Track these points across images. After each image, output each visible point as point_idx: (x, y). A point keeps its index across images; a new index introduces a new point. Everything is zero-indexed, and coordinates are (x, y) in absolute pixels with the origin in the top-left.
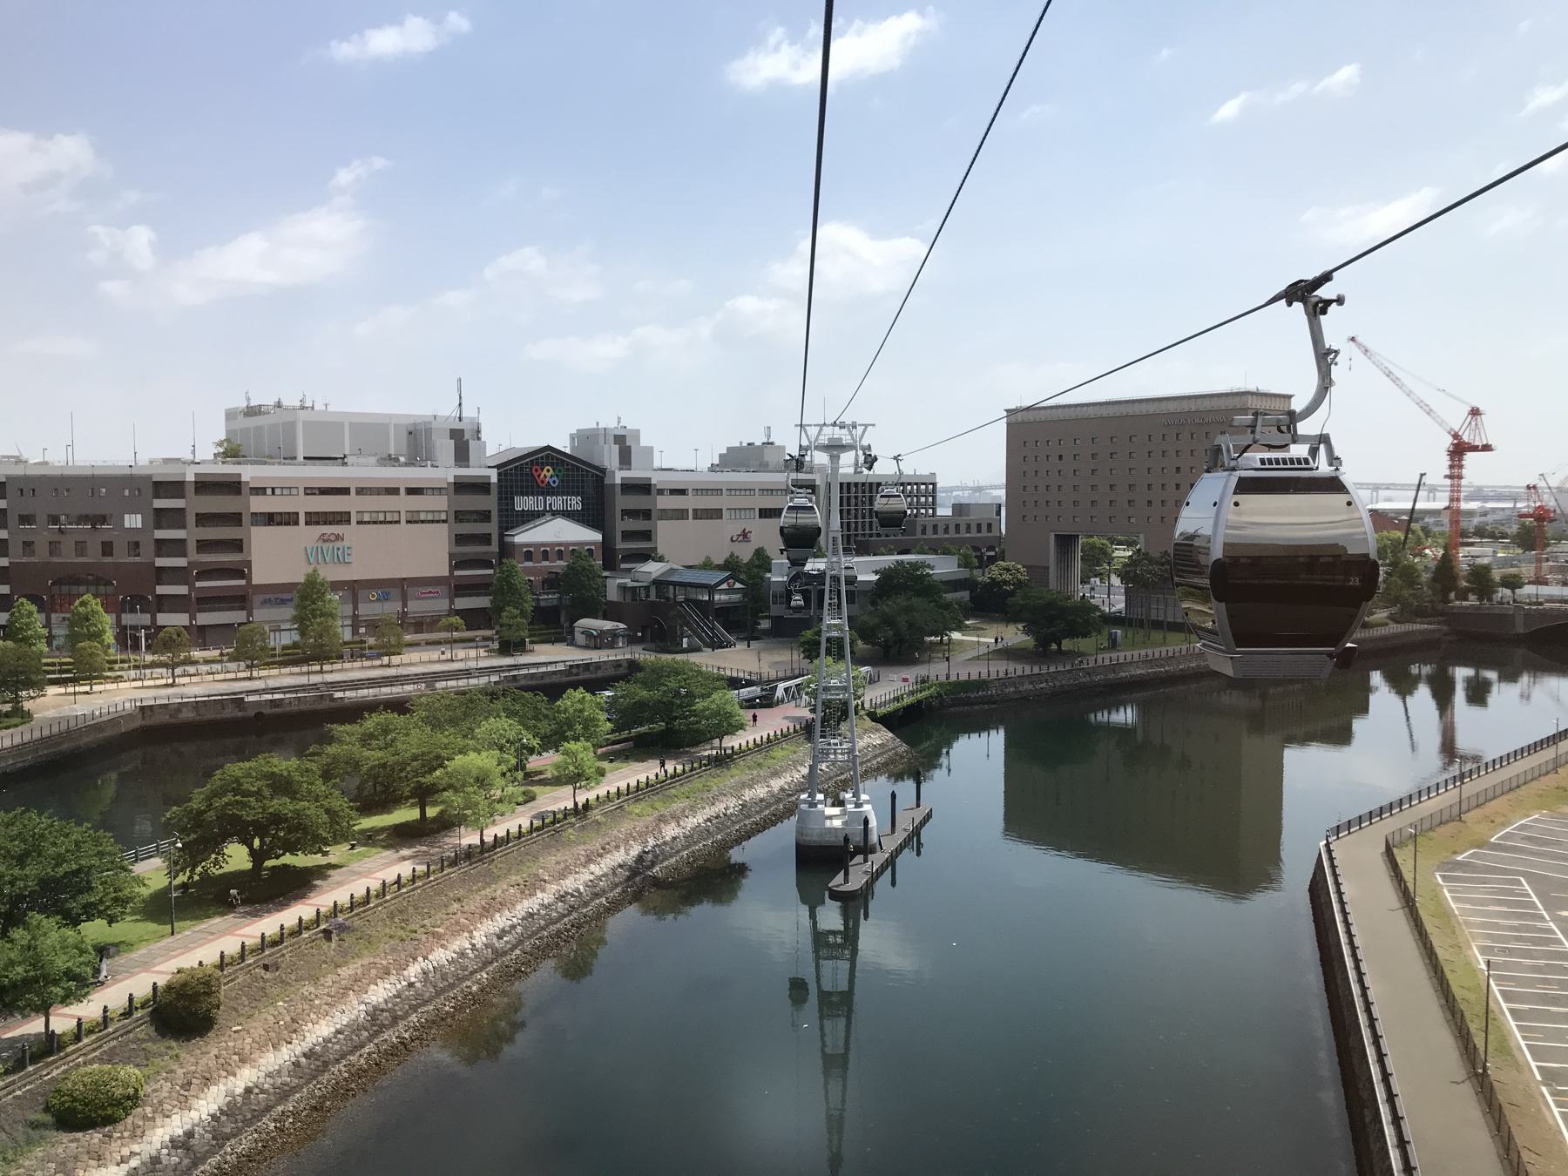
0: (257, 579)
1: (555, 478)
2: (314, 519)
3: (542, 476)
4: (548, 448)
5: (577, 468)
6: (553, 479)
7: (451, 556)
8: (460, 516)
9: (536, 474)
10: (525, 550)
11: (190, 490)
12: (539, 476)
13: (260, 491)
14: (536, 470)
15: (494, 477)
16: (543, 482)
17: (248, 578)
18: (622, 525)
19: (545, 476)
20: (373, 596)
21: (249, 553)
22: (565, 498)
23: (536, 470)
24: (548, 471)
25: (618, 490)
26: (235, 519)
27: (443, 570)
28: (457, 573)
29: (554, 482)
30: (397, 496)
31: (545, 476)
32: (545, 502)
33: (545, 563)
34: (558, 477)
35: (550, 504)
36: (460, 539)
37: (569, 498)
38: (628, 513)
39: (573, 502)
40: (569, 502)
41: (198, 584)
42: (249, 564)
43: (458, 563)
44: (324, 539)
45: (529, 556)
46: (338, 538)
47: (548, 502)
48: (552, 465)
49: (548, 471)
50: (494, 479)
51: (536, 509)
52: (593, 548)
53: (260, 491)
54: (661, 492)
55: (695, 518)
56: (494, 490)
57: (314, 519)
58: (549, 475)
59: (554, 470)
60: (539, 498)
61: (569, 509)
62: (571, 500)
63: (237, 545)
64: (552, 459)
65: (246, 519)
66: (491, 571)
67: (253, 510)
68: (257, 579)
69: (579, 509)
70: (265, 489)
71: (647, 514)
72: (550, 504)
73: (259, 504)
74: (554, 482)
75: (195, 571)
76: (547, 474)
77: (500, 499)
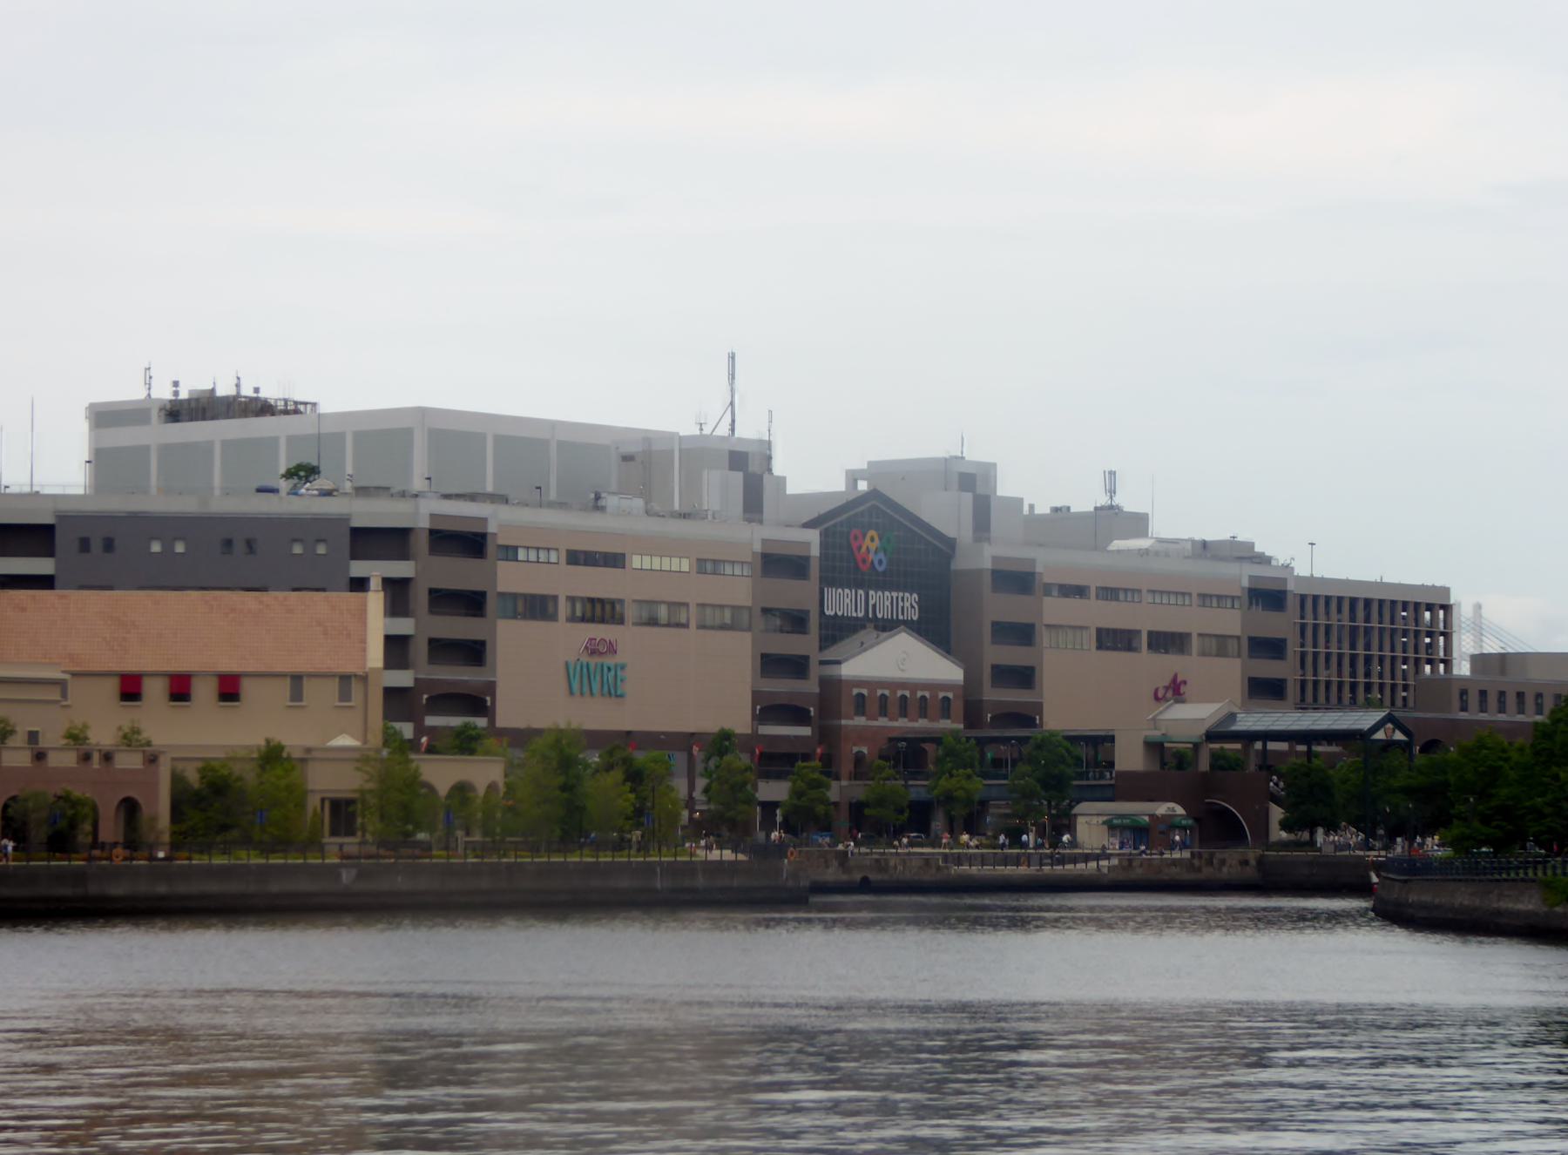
0: (501, 723)
1: (881, 555)
3: (863, 550)
7: (756, 696)
10: (855, 691)
11: (421, 544)
12: (860, 548)
13: (510, 552)
16: (864, 561)
21: (495, 676)
24: (872, 539)
27: (739, 720)
29: (880, 562)
31: (868, 548)
33: (883, 722)
37: (901, 594)
40: (901, 604)
41: (431, 721)
42: (491, 687)
43: (769, 710)
44: (593, 650)
45: (861, 705)
47: (871, 602)
50: (815, 551)
52: (950, 695)
54: (1047, 589)
58: (873, 546)
62: (903, 600)
63: (474, 652)
65: (491, 604)
66: (805, 731)
68: (501, 723)
69: (915, 618)
70: (515, 549)
72: (874, 606)
74: (880, 562)
75: (425, 696)
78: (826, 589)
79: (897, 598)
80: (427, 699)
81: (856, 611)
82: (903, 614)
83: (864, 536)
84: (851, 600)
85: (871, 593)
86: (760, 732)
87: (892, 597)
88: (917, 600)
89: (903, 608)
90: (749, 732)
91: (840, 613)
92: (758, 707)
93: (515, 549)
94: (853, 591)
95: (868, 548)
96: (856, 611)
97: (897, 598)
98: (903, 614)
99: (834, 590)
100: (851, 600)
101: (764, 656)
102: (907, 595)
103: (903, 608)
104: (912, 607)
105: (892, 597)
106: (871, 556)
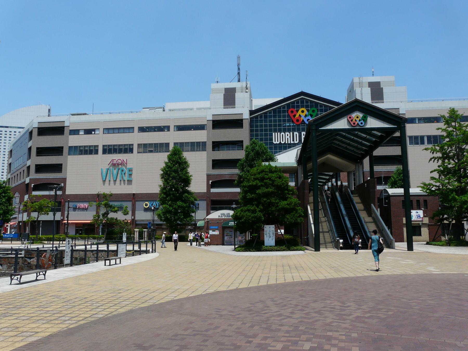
0: (69, 191)
2: (108, 150)
4: (302, 93)
7: (209, 177)
8: (217, 145)
9: (291, 115)
12: (295, 116)
14: (292, 112)
15: (246, 116)
17: (63, 189)
20: (146, 205)
23: (292, 112)
24: (303, 112)
26: (58, 151)
28: (213, 190)
31: (300, 115)
32: (300, 136)
36: (217, 164)
41: (34, 193)
42: (64, 180)
44: (114, 165)
46: (123, 163)
48: (307, 107)
51: (292, 142)
53: (75, 132)
56: (246, 124)
57: (108, 150)
58: (303, 115)
59: (308, 111)
60: (295, 133)
63: (58, 168)
64: (307, 102)
65: (66, 151)
67: (70, 145)
68: (69, 191)
73: (74, 141)
75: (33, 185)
76: (301, 114)
77: (251, 131)
78: (274, 134)
80: (33, 186)
81: (293, 140)
83: (297, 111)
84: (290, 137)
86: (211, 191)
90: (205, 191)
91: (282, 142)
92: (211, 181)
94: (291, 133)
95: (300, 115)
96: (293, 140)
99: (279, 133)
100: (290, 137)
101: (213, 161)
106: (302, 119)
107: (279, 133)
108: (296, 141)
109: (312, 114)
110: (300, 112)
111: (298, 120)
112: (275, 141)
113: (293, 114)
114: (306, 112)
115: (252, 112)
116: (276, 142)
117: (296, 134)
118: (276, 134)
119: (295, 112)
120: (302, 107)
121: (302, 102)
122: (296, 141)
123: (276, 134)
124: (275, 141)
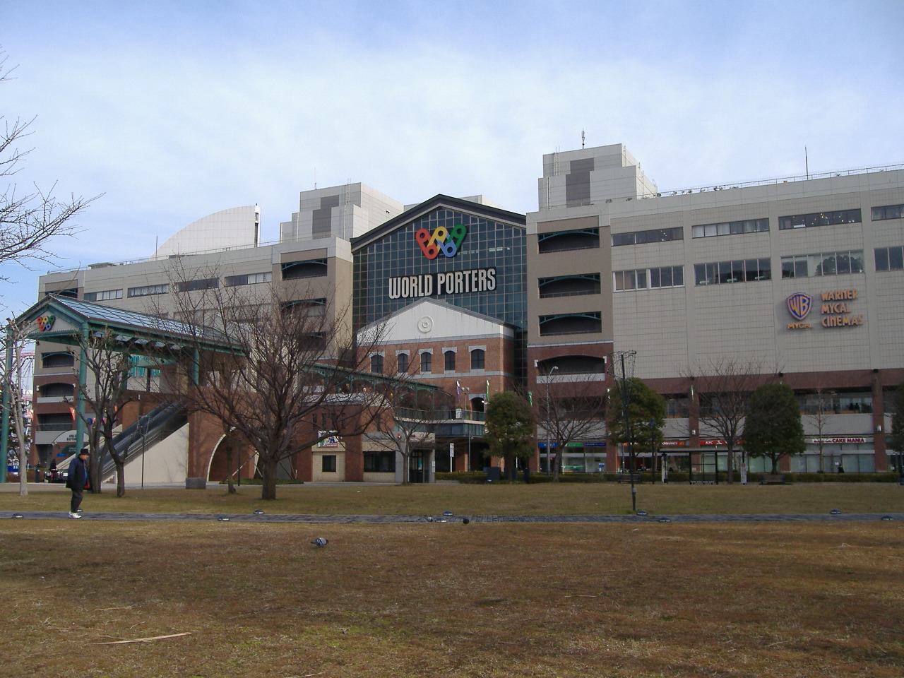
1: (451, 244)
3: (431, 243)
4: (440, 198)
5: (491, 223)
6: (448, 245)
12: (426, 243)
13: (91, 297)
18: (538, 307)
19: (435, 241)
22: (467, 273)
23: (422, 235)
24: (441, 233)
25: (533, 245)
30: (602, 313)
31: (435, 241)
34: (455, 240)
35: (443, 286)
38: (550, 287)
39: (481, 279)
40: (474, 279)
47: (440, 283)
49: (441, 233)
54: (624, 239)
55: (655, 283)
58: (441, 239)
59: (450, 231)
60: (426, 277)
61: (474, 289)
62: (477, 275)
70: (95, 294)
71: (589, 283)
72: (443, 286)
74: (450, 250)
78: (390, 280)
79: (470, 275)
81: (423, 291)
82: (477, 286)
84: (418, 285)
85: (439, 276)
87: (464, 276)
88: (494, 273)
89: (477, 283)
93: (95, 294)
94: (420, 277)
96: (423, 291)
97: (470, 275)
98: (477, 286)
99: (399, 279)
100: (418, 285)
102: (480, 272)
103: (477, 283)
104: (488, 279)
105: (464, 276)
107: (399, 279)
108: (428, 291)
109: (457, 236)
110: (435, 235)
111: (431, 251)
112: (393, 295)
113: (425, 240)
114: (445, 233)
115: (354, 242)
116: (395, 296)
117: (428, 279)
118: (395, 279)
119: (427, 234)
120: (441, 224)
121: (442, 215)
122: (428, 291)
123: (395, 279)
124: (393, 295)
